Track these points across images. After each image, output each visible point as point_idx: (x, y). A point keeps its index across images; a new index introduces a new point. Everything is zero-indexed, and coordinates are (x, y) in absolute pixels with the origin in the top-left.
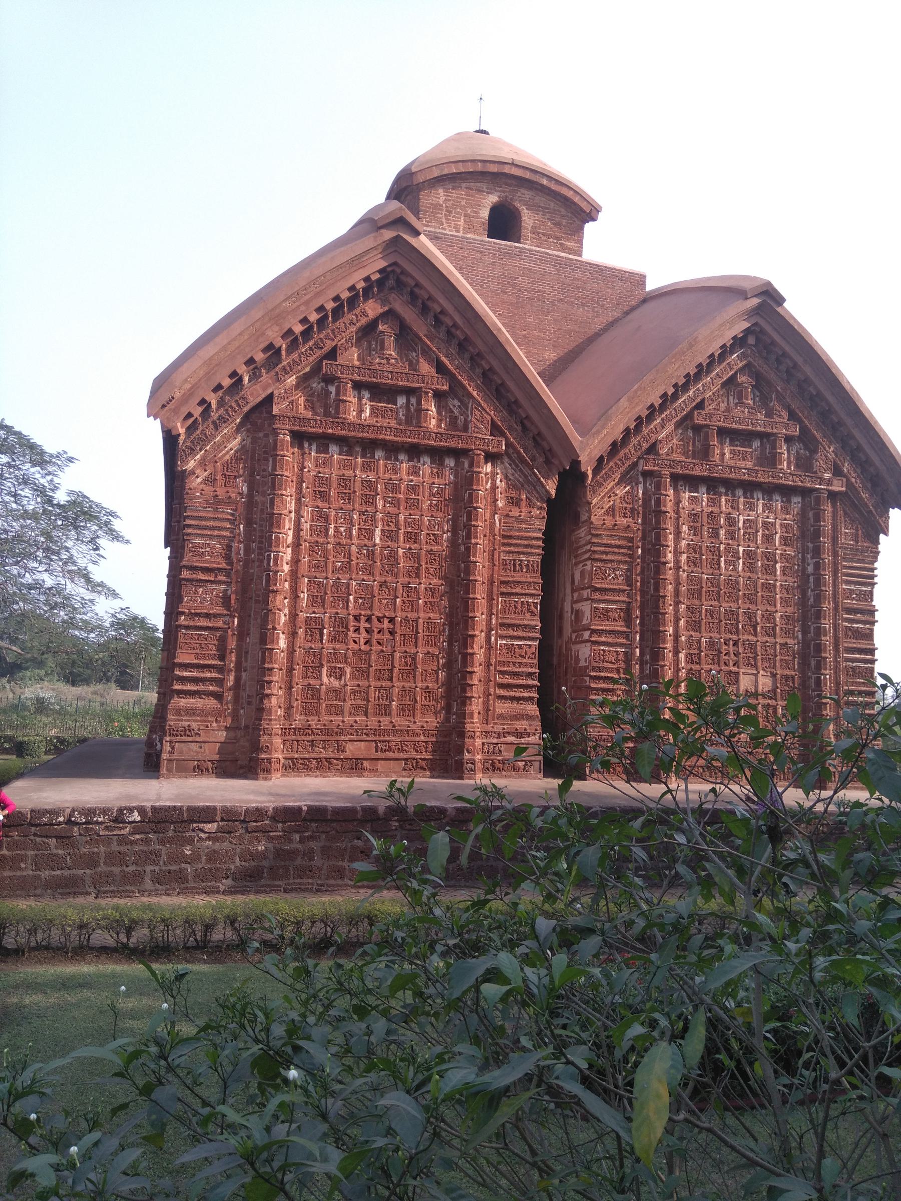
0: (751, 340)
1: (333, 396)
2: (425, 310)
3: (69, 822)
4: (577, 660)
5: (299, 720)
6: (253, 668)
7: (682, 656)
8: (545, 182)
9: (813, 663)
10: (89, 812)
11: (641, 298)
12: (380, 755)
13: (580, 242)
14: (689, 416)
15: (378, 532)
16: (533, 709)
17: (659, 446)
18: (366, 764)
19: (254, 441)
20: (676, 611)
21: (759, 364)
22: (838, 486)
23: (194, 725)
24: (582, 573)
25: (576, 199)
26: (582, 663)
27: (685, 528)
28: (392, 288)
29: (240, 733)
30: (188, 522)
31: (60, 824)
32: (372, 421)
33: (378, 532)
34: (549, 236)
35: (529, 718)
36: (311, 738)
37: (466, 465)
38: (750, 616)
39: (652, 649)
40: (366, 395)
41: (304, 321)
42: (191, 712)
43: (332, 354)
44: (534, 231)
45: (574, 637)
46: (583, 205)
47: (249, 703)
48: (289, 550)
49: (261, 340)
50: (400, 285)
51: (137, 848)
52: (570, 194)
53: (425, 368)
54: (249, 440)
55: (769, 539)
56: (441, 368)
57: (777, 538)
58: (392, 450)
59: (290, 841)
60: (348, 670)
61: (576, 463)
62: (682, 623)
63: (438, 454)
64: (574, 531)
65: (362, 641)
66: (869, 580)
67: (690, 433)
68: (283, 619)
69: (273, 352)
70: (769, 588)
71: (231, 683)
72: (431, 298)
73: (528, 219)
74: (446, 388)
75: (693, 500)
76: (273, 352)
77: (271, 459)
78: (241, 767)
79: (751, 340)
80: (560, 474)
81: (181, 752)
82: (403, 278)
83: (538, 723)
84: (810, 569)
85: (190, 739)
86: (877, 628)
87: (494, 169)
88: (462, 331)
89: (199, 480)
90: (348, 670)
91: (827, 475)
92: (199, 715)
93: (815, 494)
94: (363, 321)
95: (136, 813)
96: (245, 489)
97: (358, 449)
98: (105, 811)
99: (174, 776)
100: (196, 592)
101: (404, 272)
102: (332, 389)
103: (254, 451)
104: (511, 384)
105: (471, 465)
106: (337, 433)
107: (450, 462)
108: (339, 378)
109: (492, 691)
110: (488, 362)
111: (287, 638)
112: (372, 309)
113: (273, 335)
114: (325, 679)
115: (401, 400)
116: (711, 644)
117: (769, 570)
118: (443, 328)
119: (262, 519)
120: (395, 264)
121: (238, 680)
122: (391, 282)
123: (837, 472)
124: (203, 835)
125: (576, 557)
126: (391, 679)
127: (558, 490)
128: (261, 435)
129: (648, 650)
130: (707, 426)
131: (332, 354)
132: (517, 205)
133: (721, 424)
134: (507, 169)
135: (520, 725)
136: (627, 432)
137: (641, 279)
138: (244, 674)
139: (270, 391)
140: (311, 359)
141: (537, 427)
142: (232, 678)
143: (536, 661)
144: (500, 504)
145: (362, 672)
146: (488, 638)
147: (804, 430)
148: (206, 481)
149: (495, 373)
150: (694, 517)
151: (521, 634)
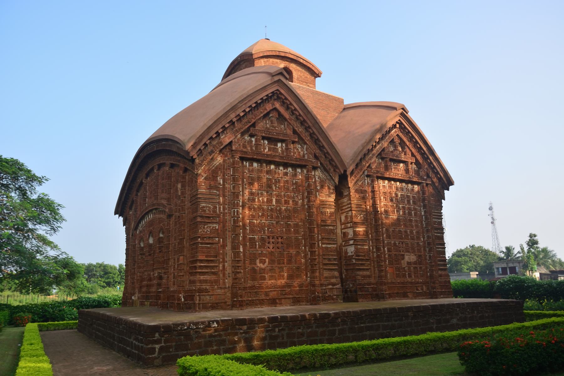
0: (398, 126)
1: (254, 142)
2: (288, 108)
3: (188, 328)
4: (346, 253)
5: (250, 283)
6: (229, 261)
7: (386, 249)
8: (301, 61)
9: (427, 249)
10: (196, 324)
11: (343, 108)
12: (283, 297)
13: (315, 85)
14: (380, 154)
15: (274, 200)
16: (336, 274)
17: (372, 165)
18: (277, 301)
19: (224, 161)
20: (382, 231)
21: (401, 134)
22: (429, 182)
23: (208, 287)
24: (346, 217)
25: (313, 69)
26: (350, 254)
27: (382, 198)
28: (275, 100)
29: (226, 290)
30: (199, 196)
31: (185, 330)
32: (269, 153)
33: (274, 200)
34: (304, 82)
35: (336, 277)
36: (256, 290)
37: (305, 172)
38: (406, 232)
39: (376, 246)
40: (266, 142)
41: (244, 111)
42: (206, 281)
43: (254, 125)
44: (298, 79)
45: (343, 243)
46: (316, 71)
47: (229, 277)
48: (241, 208)
49: (228, 118)
50: (278, 98)
51: (216, 339)
52: (311, 66)
53: (290, 132)
54: (222, 160)
55: (409, 202)
56: (295, 132)
57: (411, 201)
58: (277, 164)
59: (275, 331)
60: (267, 260)
61: (345, 171)
62: (385, 236)
63: (294, 167)
64: (340, 199)
65: (271, 247)
66: (440, 216)
67: (380, 161)
68: (241, 238)
69: (232, 123)
70: (411, 221)
71: (221, 268)
72: (291, 104)
73: (295, 75)
74: (297, 140)
75: (384, 186)
76: (232, 123)
77: (232, 169)
78: (229, 305)
79: (398, 126)
80: (339, 176)
81: (203, 300)
82: (280, 95)
83: (339, 279)
84: (423, 213)
85: (207, 294)
86: (445, 235)
87: (283, 54)
88: (302, 117)
89: (203, 178)
90: (267, 260)
91: (425, 177)
92: (209, 283)
93: (422, 184)
94: (266, 112)
95: (215, 323)
96: (221, 182)
97: (265, 165)
98: (203, 323)
99: (201, 311)
100: (204, 228)
101: (281, 93)
102: (253, 139)
103: (224, 165)
104: (321, 139)
105: (307, 172)
106: (258, 158)
107: (299, 170)
108: (256, 135)
109: (321, 267)
110: (312, 130)
111: (243, 247)
112: (269, 107)
113: (232, 116)
114: (258, 265)
115: (279, 145)
116: (395, 244)
117: (410, 214)
118: (294, 116)
119: (229, 195)
120: (277, 90)
121: (224, 266)
122: (275, 97)
123: (428, 176)
124: (242, 331)
125: (342, 210)
126: (284, 263)
127: (339, 182)
128: (226, 158)
129: (374, 247)
130: (386, 158)
131: (254, 125)
132: (291, 69)
133: (391, 157)
134: (287, 55)
135: (333, 280)
136: (361, 160)
137: (342, 101)
138: (226, 264)
139: (230, 140)
140: (247, 127)
141: (331, 157)
142: (221, 266)
143: (335, 253)
144: (318, 188)
145: (272, 262)
146: (318, 244)
147: (417, 160)
148: (205, 178)
149: (315, 134)
150: (385, 193)
151: (331, 242)
